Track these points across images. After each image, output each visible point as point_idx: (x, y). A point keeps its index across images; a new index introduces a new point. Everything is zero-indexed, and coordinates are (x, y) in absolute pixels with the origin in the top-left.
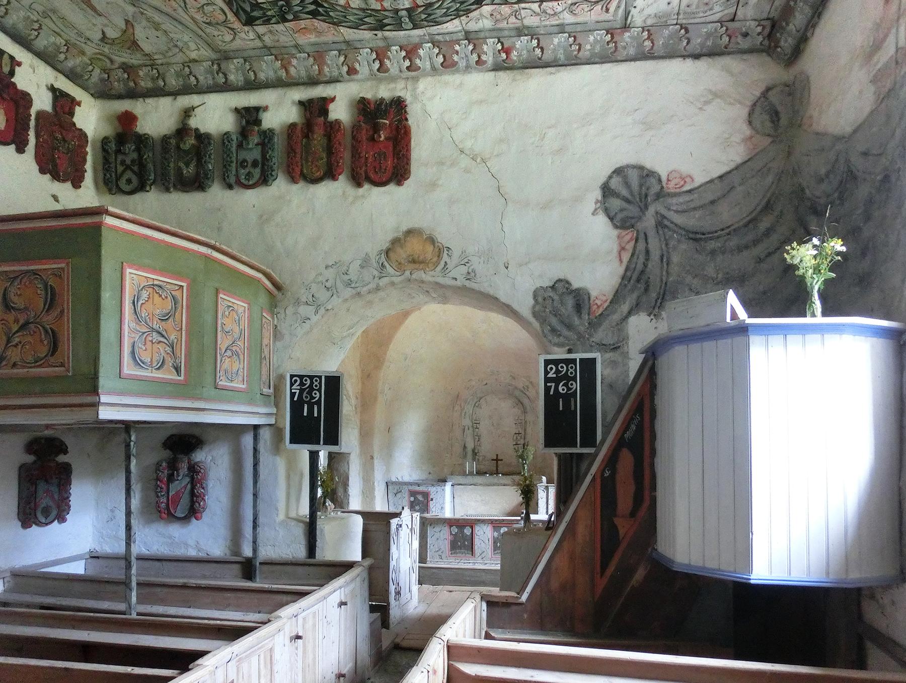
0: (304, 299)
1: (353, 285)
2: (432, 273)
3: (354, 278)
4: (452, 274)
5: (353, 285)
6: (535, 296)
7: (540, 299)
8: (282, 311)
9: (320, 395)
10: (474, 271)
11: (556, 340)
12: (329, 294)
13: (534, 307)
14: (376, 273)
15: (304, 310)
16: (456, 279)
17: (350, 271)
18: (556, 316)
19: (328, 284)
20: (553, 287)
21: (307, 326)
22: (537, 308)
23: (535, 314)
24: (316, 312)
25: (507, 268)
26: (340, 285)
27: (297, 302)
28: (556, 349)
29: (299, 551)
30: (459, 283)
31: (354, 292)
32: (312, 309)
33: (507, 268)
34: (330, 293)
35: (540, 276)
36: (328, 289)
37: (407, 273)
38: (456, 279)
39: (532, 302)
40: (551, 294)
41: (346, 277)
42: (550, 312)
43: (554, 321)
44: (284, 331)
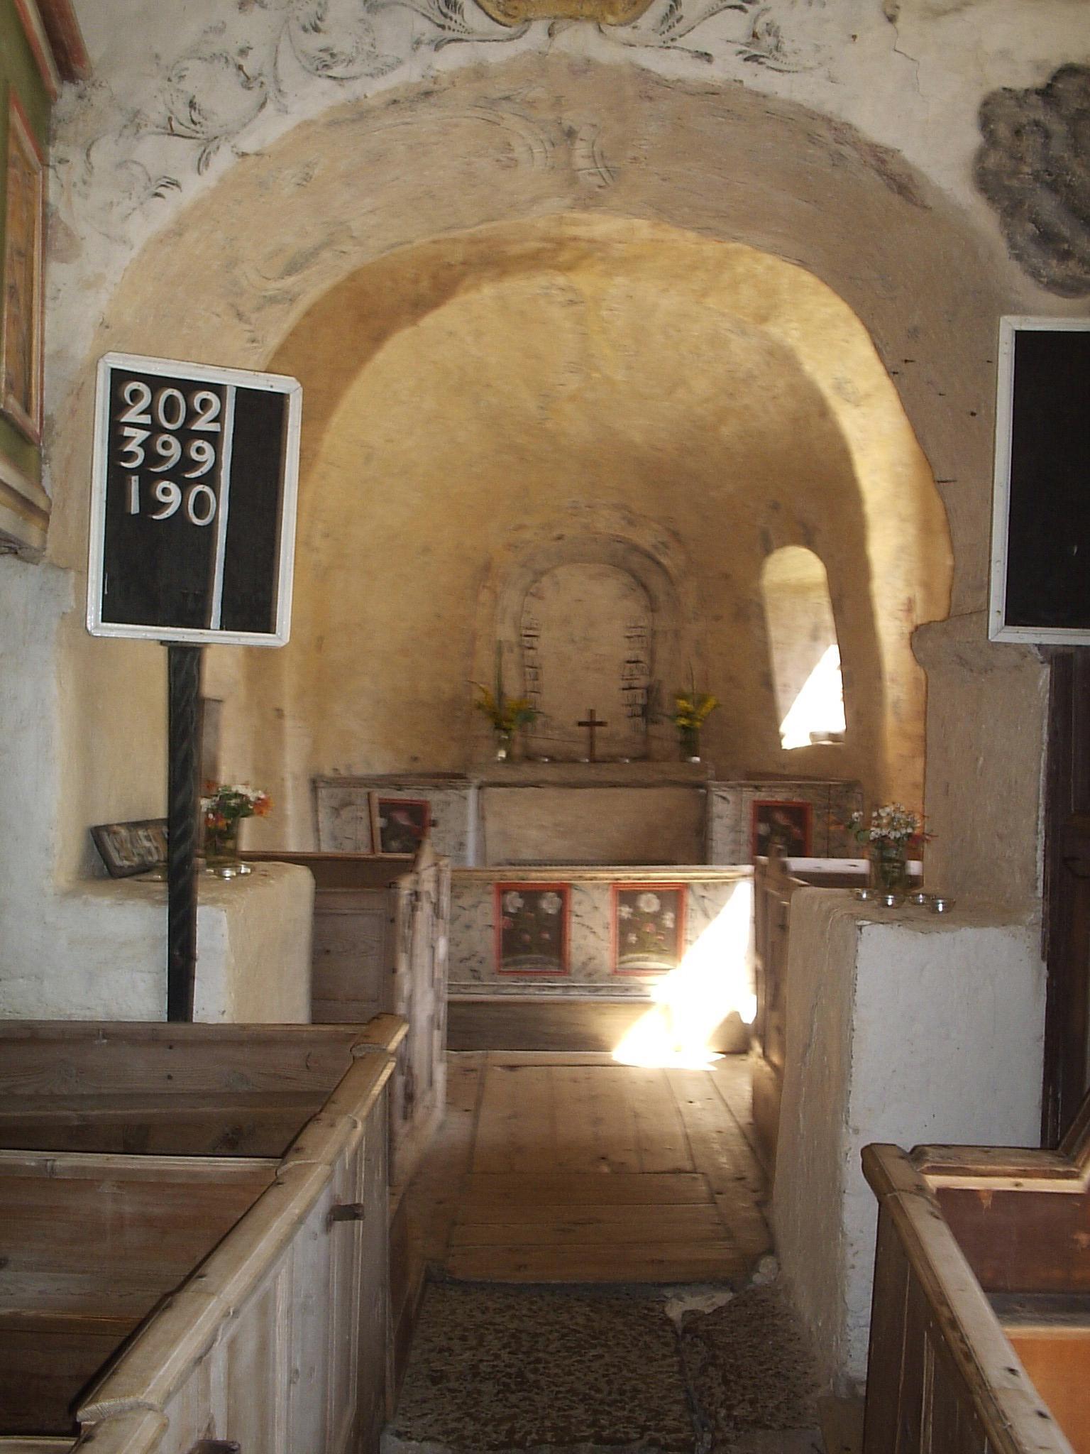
0: (156, 113)
1: (337, 71)
2: (624, 33)
3: (344, 45)
4: (696, 40)
5: (337, 71)
6: (986, 120)
7: (1003, 131)
8: (76, 158)
9: (217, 458)
10: (771, 30)
11: (1055, 269)
12: (253, 97)
13: (981, 156)
14: (427, 29)
15: (155, 152)
16: (707, 57)
17: (330, 17)
18: (1053, 188)
19: (250, 66)
20: (1047, 93)
21: (165, 212)
22: (992, 161)
23: (986, 181)
24: (202, 163)
25: (891, 19)
26: (287, 64)
27: (135, 122)
28: (1052, 299)
29: (137, 996)
30: (713, 74)
31: (341, 95)
32: (183, 151)
33: (891, 19)
34: (253, 97)
35: (1004, 54)
36: (247, 83)
37: (537, 32)
38: (707, 57)
39: (973, 138)
40: (1040, 115)
41: (314, 43)
42: (1036, 177)
43: (1048, 205)
44: (82, 229)
